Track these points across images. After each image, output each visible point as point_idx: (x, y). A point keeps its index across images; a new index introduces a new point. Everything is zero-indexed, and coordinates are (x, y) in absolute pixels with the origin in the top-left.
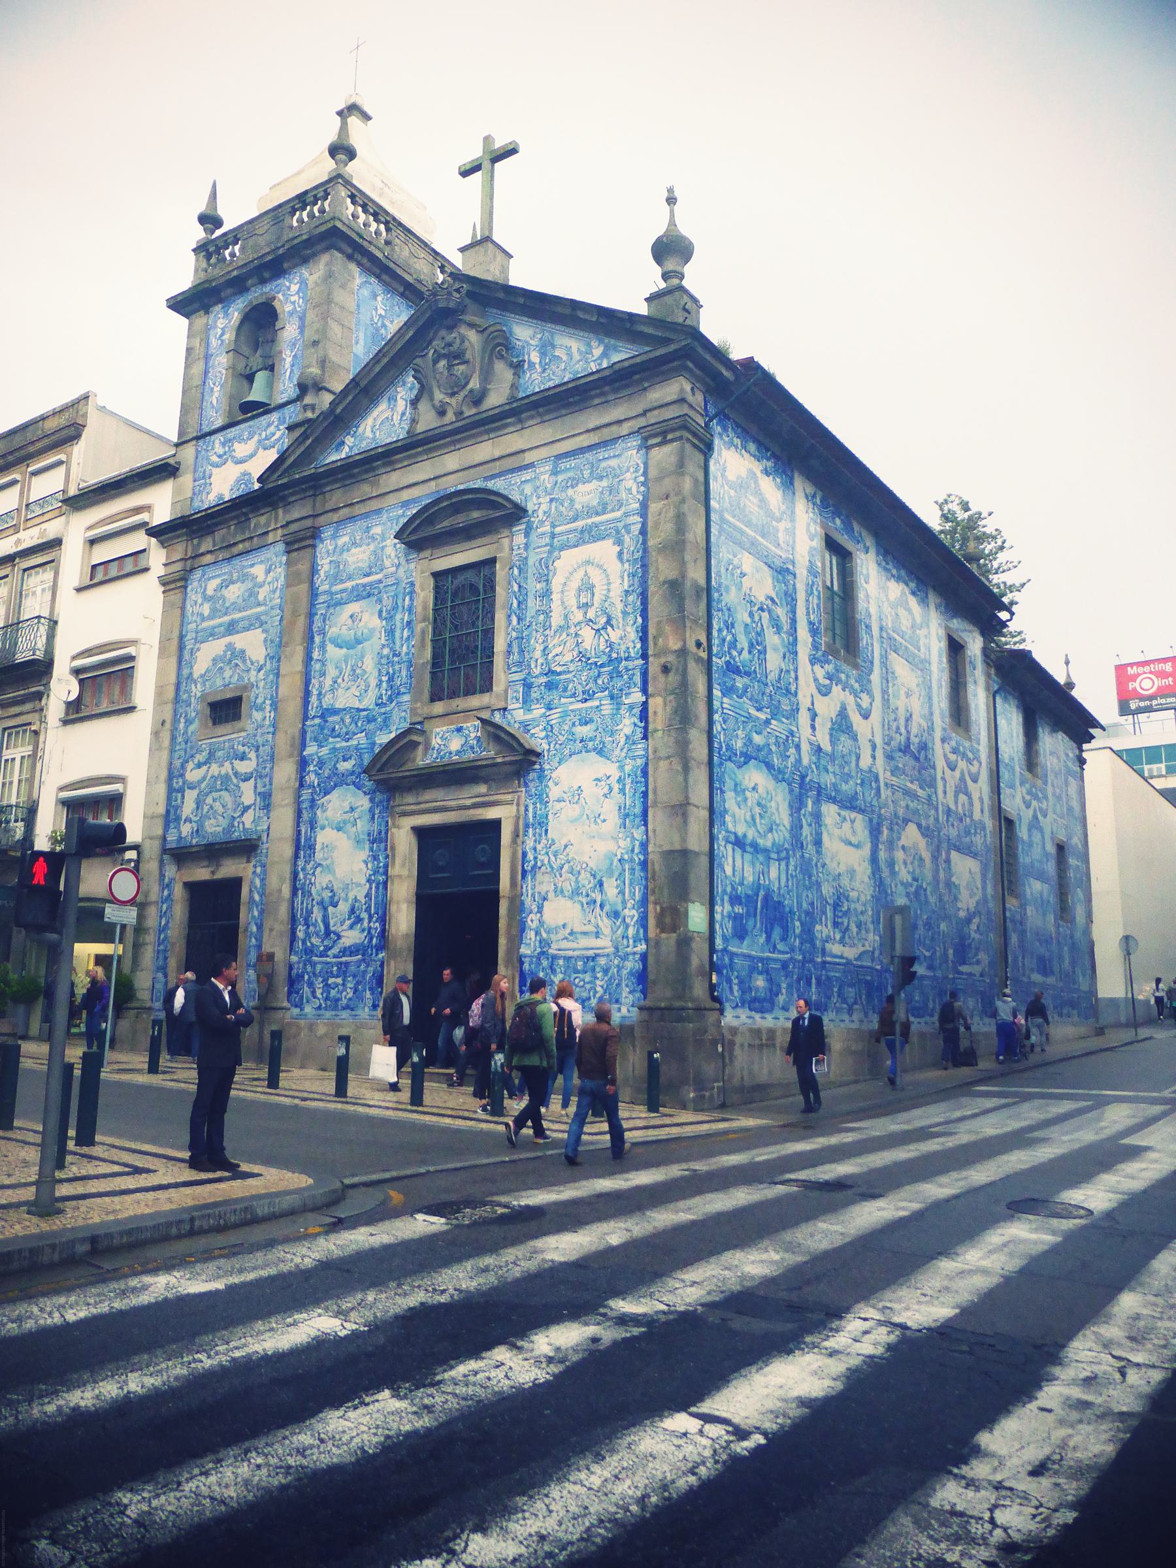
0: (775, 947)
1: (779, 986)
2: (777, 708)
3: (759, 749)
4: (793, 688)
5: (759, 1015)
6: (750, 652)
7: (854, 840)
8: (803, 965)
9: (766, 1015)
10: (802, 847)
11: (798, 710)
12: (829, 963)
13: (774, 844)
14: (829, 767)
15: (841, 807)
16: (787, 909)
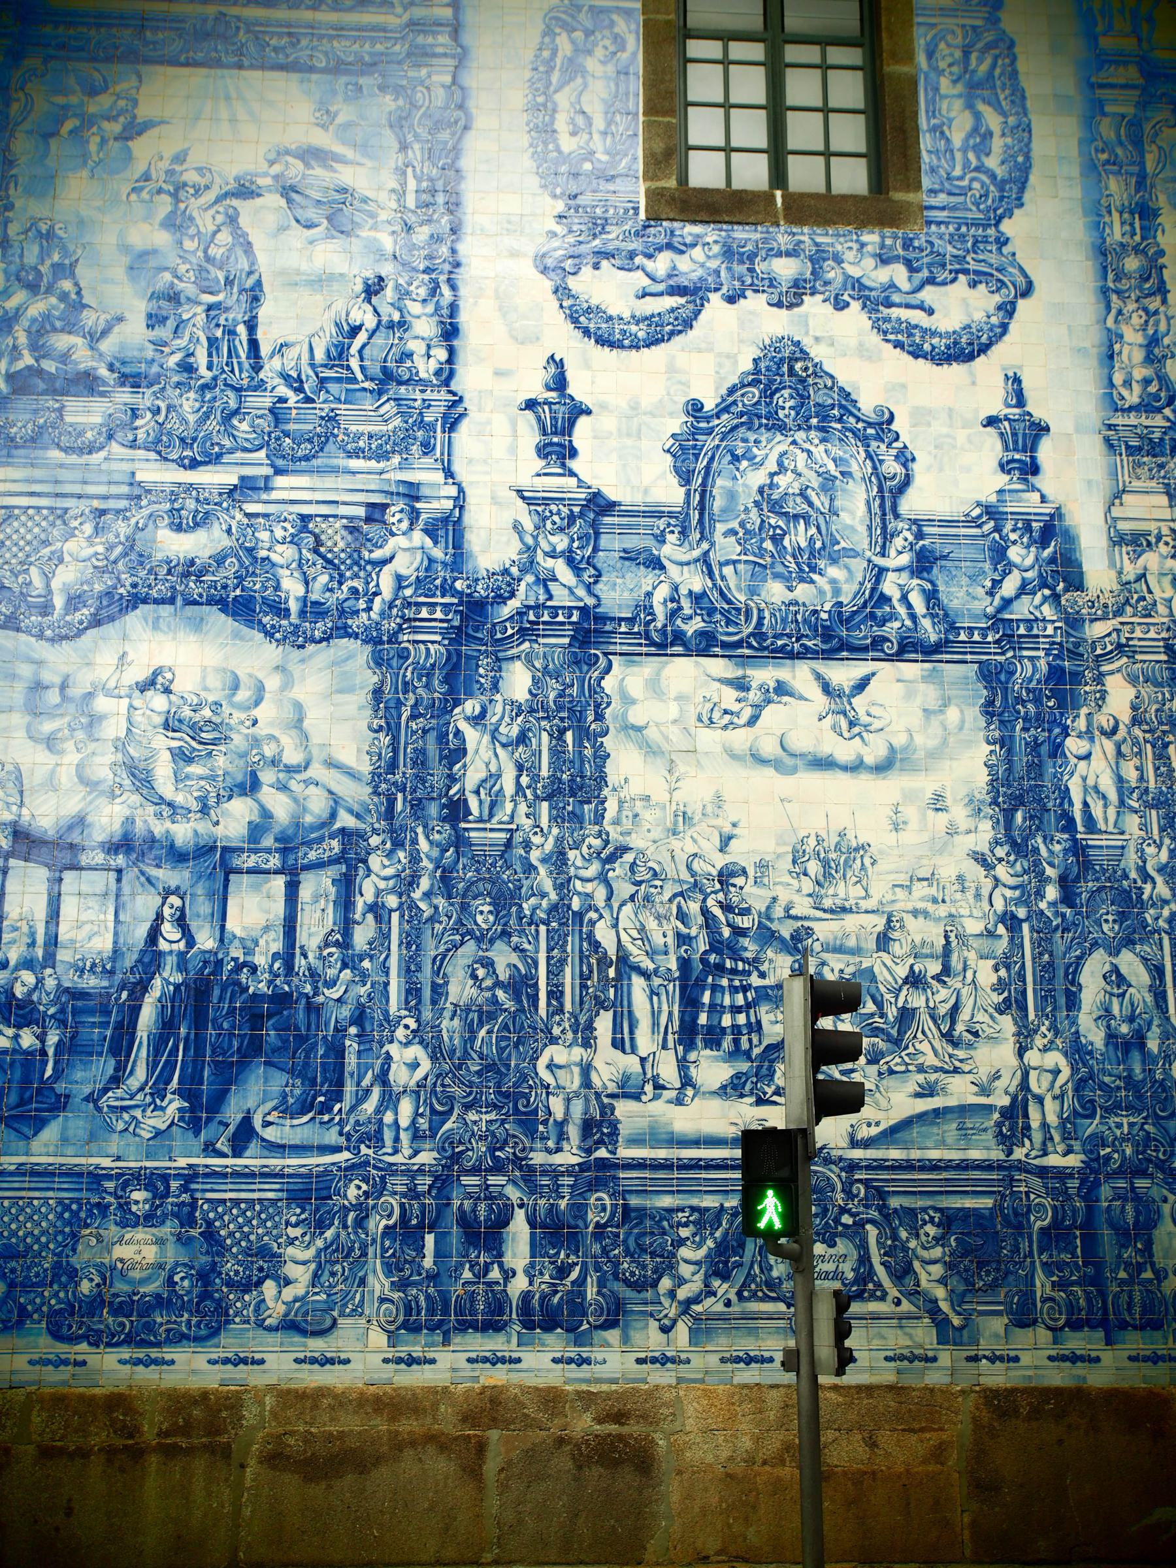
0: (244, 1135)
1: (264, 1252)
2: (328, 437)
3: (190, 569)
4: (426, 369)
5: (126, 1353)
6: (154, 320)
7: (845, 751)
8: (443, 1181)
9: (168, 1353)
10: (456, 811)
11: (452, 423)
12: (641, 1165)
13: (256, 831)
14: (669, 550)
15: (744, 661)
16: (345, 1012)
